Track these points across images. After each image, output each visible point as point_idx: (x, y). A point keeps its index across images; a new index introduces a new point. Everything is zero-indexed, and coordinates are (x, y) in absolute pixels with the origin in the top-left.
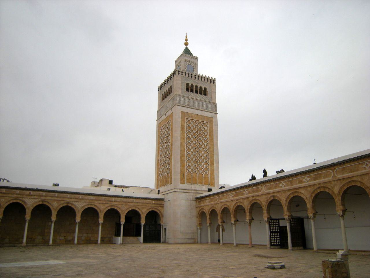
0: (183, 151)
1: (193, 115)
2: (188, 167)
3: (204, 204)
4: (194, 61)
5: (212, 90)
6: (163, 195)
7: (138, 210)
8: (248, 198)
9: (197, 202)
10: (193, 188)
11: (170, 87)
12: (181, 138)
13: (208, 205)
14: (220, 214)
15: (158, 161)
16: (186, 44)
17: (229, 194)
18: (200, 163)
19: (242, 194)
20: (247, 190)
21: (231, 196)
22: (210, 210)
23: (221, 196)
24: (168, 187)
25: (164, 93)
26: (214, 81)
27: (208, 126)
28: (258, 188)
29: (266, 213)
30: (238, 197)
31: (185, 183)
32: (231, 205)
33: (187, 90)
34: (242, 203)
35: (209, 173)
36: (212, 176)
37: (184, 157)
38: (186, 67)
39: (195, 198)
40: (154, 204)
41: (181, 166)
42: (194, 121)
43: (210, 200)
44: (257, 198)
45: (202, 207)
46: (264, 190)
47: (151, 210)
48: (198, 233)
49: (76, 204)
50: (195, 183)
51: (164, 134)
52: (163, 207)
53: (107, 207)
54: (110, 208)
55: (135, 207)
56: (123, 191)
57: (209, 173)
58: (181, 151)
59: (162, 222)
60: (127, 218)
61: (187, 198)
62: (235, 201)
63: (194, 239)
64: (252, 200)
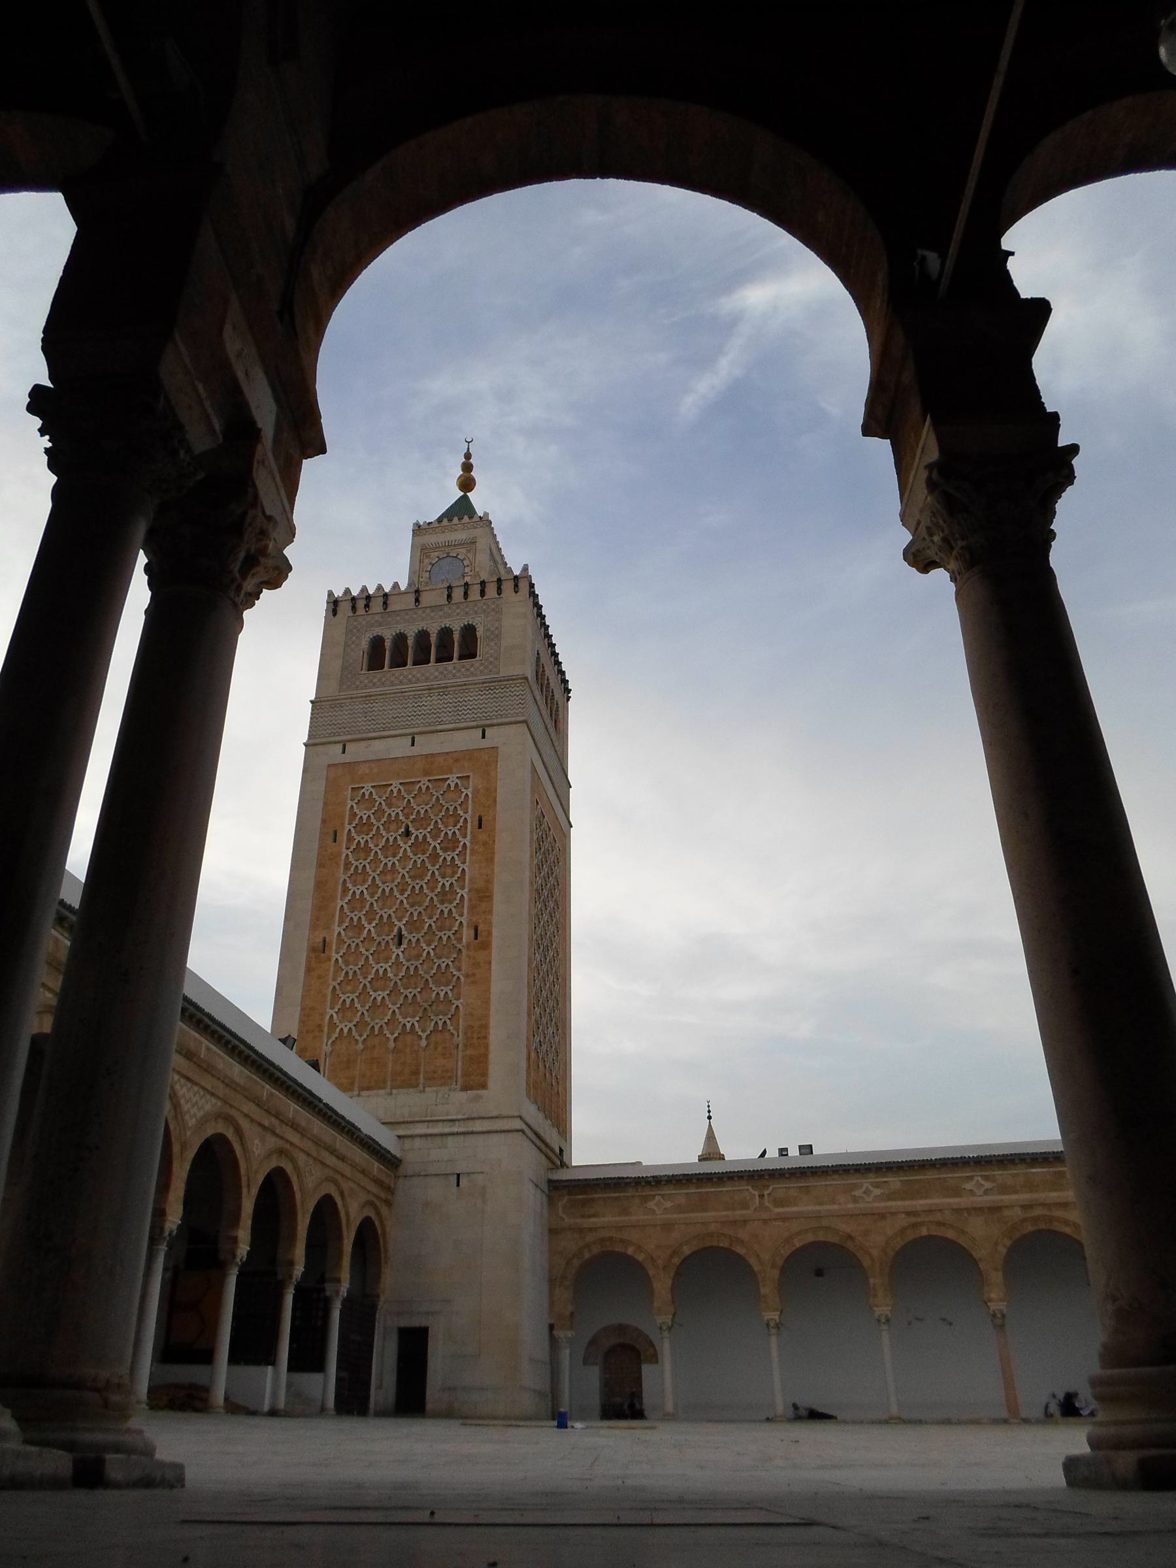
6: (399, 1137)
8: (995, 1209)
13: (667, 1226)
14: (776, 1273)
15: (320, 950)
16: (467, 484)
17: (854, 1187)
19: (957, 1192)
20: (986, 1178)
22: (687, 1251)
23: (778, 1188)
24: (457, 1101)
25: (388, 635)
30: (922, 1202)
34: (951, 1226)
39: (550, 1181)
43: (682, 1200)
45: (606, 1234)
49: (183, 1090)
51: (388, 830)
52: (388, 1203)
55: (336, 1183)
62: (903, 1216)
64: (1025, 1220)
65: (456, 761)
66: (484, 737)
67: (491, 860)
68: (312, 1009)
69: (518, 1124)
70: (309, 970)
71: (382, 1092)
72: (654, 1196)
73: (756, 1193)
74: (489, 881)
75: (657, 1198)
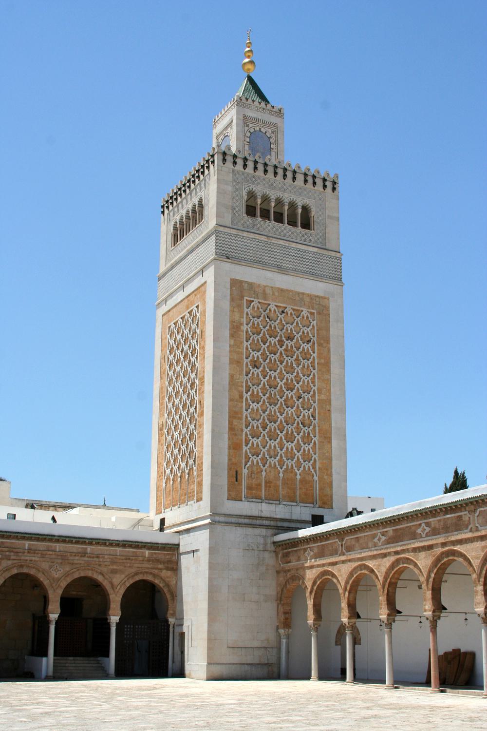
0: (237, 401)
1: (268, 291)
2: (253, 451)
3: (298, 563)
4: (273, 119)
5: (327, 212)
7: (100, 578)
9: (277, 556)
10: (266, 514)
11: (197, 203)
12: (231, 361)
14: (347, 593)
17: (374, 536)
18: (290, 438)
19: (414, 536)
20: (428, 524)
21: (379, 540)
25: (177, 218)
26: (334, 183)
27: (315, 322)
28: (460, 517)
29: (483, 593)
31: (243, 499)
32: (379, 565)
33: (251, 211)
35: (314, 468)
36: (326, 477)
37: (241, 419)
38: (248, 140)
39: (274, 543)
40: (149, 560)
41: (229, 448)
42: (270, 310)
44: (457, 548)
45: (293, 572)
46: (477, 525)
47: (138, 578)
48: (279, 649)
50: (273, 498)
53: (8, 569)
54: (15, 571)
56: (53, 519)
57: (314, 468)
58: (231, 400)
59: (174, 615)
60: (69, 604)
61: (249, 545)
63: (268, 665)
65: (196, 295)
66: (203, 276)
67: (204, 357)
68: (160, 463)
69: (208, 521)
70: (159, 441)
71: (176, 507)
72: (307, 548)
73: (340, 543)
74: (204, 372)
75: (309, 549)
